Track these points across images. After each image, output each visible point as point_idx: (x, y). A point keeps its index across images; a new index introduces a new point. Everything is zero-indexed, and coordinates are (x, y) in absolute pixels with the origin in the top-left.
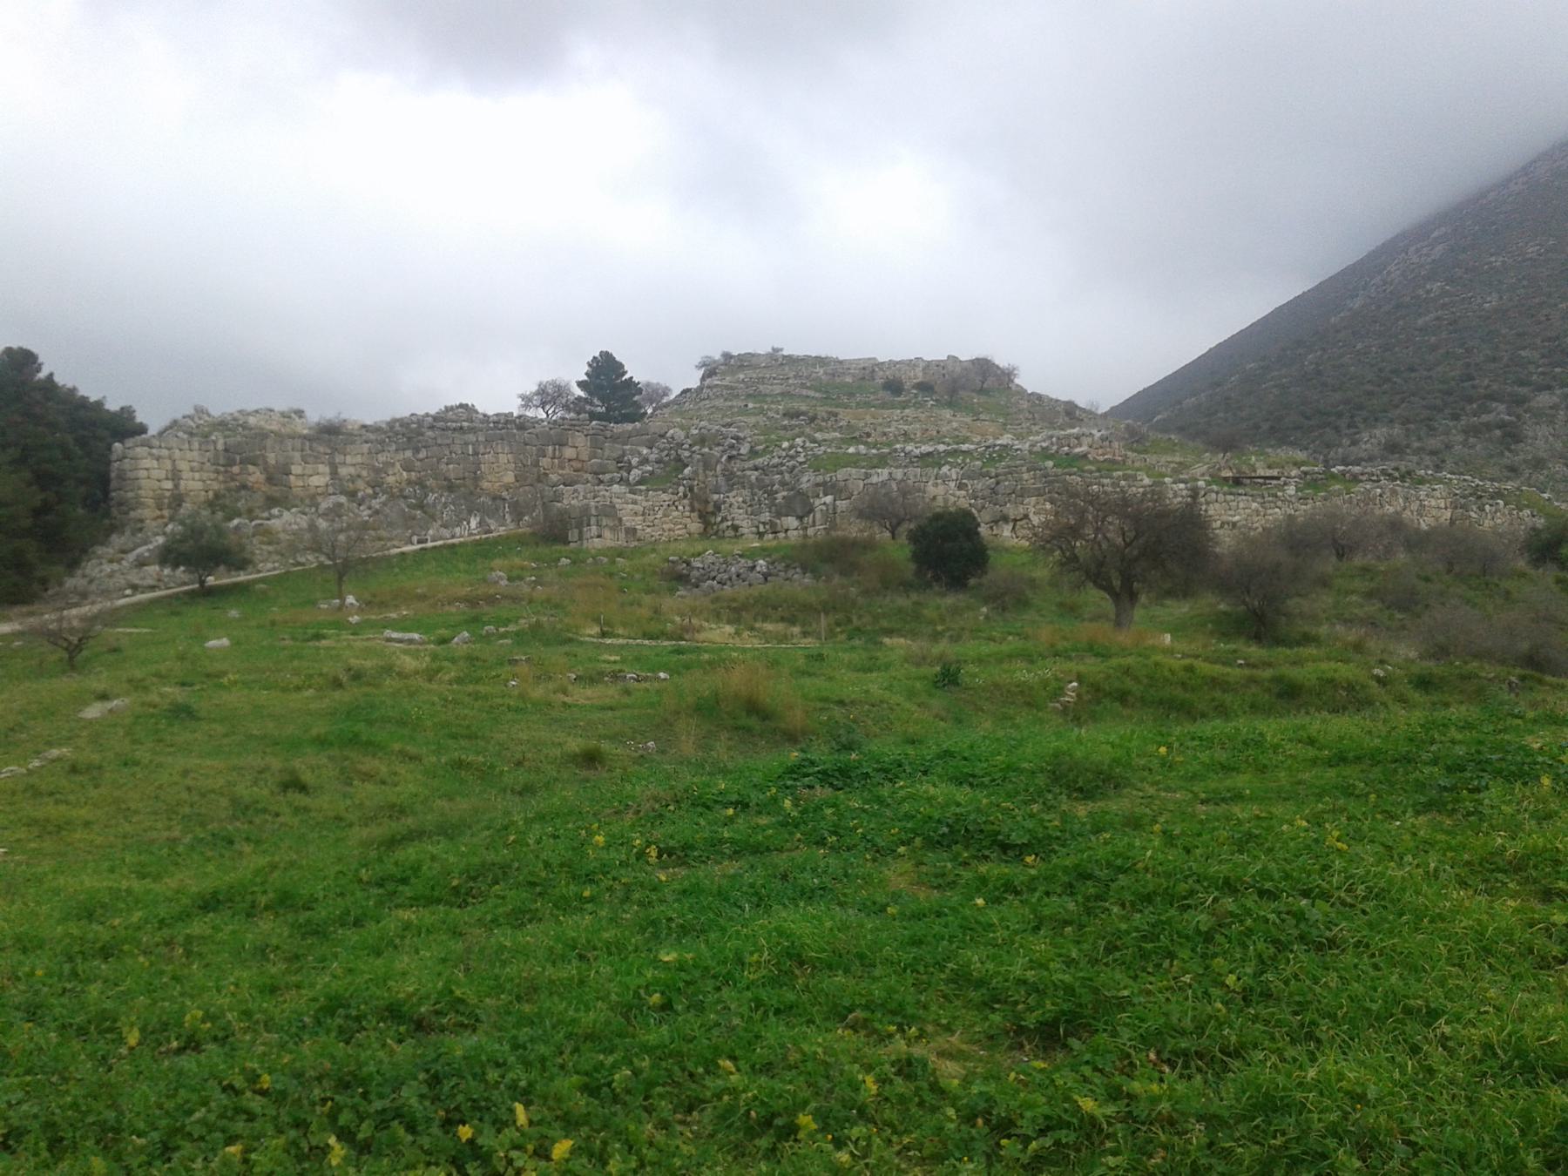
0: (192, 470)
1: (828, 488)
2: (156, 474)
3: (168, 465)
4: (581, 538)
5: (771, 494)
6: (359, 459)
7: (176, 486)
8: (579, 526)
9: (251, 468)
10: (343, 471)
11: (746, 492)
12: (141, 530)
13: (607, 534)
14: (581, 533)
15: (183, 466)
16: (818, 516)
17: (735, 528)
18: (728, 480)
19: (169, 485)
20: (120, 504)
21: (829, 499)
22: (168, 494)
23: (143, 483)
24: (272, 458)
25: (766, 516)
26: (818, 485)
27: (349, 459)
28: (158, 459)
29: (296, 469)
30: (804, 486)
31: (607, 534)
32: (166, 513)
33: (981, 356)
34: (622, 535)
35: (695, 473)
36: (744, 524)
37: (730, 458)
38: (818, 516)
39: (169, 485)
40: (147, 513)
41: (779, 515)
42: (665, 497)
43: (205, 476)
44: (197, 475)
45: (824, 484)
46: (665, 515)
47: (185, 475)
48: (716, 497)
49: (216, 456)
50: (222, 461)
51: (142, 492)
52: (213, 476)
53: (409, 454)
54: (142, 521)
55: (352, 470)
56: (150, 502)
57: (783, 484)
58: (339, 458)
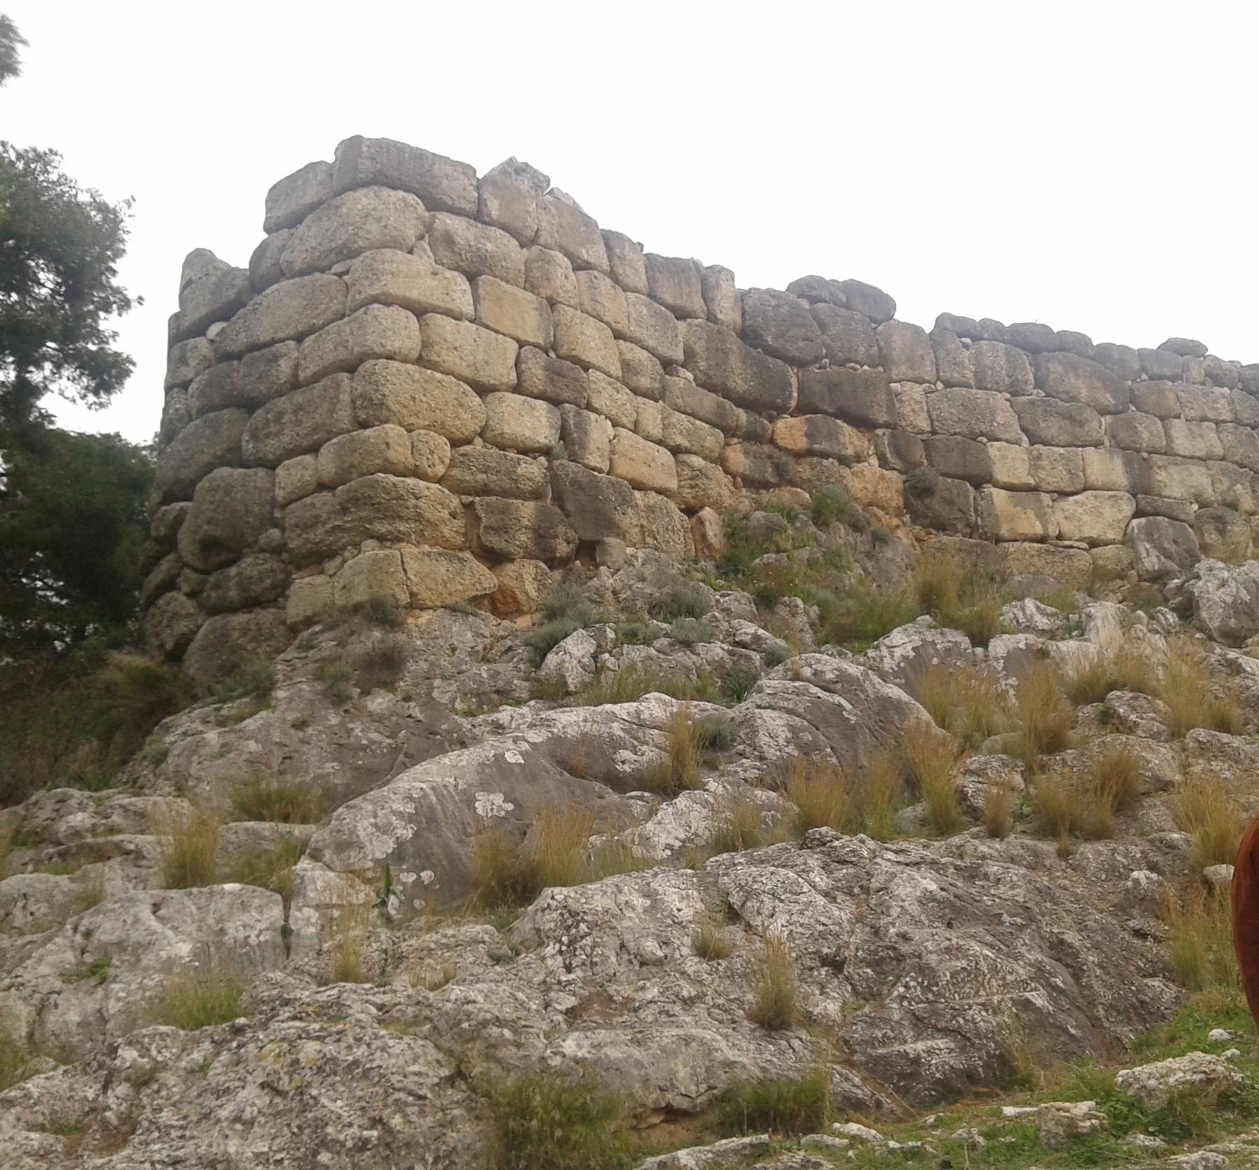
0: (628, 376)
6: (1211, 441)
9: (850, 439)
12: (384, 668)
15: (591, 341)
20: (220, 551)
22: (532, 470)
23: (399, 382)
28: (473, 270)
29: (1009, 461)
32: (526, 578)
39: (532, 422)
40: (424, 569)
44: (651, 414)
47: (607, 395)
51: (392, 438)
52: (713, 439)
54: (381, 613)
55: (1200, 479)
56: (435, 501)
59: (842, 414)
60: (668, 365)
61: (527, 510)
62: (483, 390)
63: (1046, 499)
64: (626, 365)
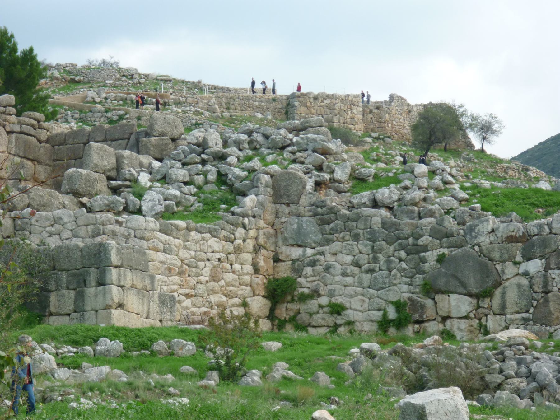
1: (530, 245)
4: (79, 309)
5: (416, 250)
8: (80, 283)
11: (364, 246)
14: (80, 296)
16: (512, 295)
17: (337, 310)
18: (323, 222)
21: (534, 266)
25: (403, 291)
26: (511, 239)
30: (485, 240)
33: (436, 100)
34: (155, 307)
35: (261, 205)
36: (355, 303)
37: (318, 185)
38: (512, 295)
41: (430, 290)
45: (525, 239)
46: (214, 278)
48: (296, 252)
57: (441, 234)
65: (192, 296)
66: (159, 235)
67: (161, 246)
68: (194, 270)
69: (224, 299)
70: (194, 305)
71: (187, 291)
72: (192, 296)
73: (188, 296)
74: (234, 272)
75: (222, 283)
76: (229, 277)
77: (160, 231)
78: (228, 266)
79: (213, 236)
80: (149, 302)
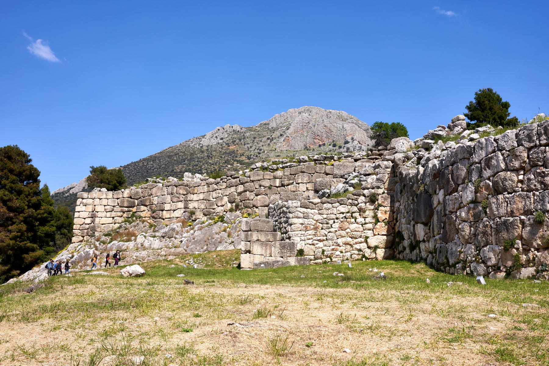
2: (83, 215)
3: (90, 208)
6: (201, 196)
7: (93, 222)
9: (143, 208)
10: (191, 206)
13: (257, 249)
15: (99, 208)
19: (88, 221)
24: (155, 200)
27: (195, 197)
31: (257, 249)
42: (342, 209)
43: (113, 214)
44: (108, 214)
49: (123, 202)
50: (126, 204)
52: (120, 214)
53: (233, 189)
58: (190, 197)
59: (142, 205)
60: (114, 206)
61: (86, 231)
62: (85, 219)
63: (172, 211)
64: (105, 210)
65: (324, 240)
66: (299, 209)
67: (301, 215)
68: (325, 225)
69: (350, 239)
70: (325, 246)
71: (319, 238)
72: (324, 240)
73: (320, 241)
74: (357, 223)
75: (348, 230)
76: (354, 226)
77: (301, 207)
78: (353, 220)
79: (341, 204)
80: (271, 248)
